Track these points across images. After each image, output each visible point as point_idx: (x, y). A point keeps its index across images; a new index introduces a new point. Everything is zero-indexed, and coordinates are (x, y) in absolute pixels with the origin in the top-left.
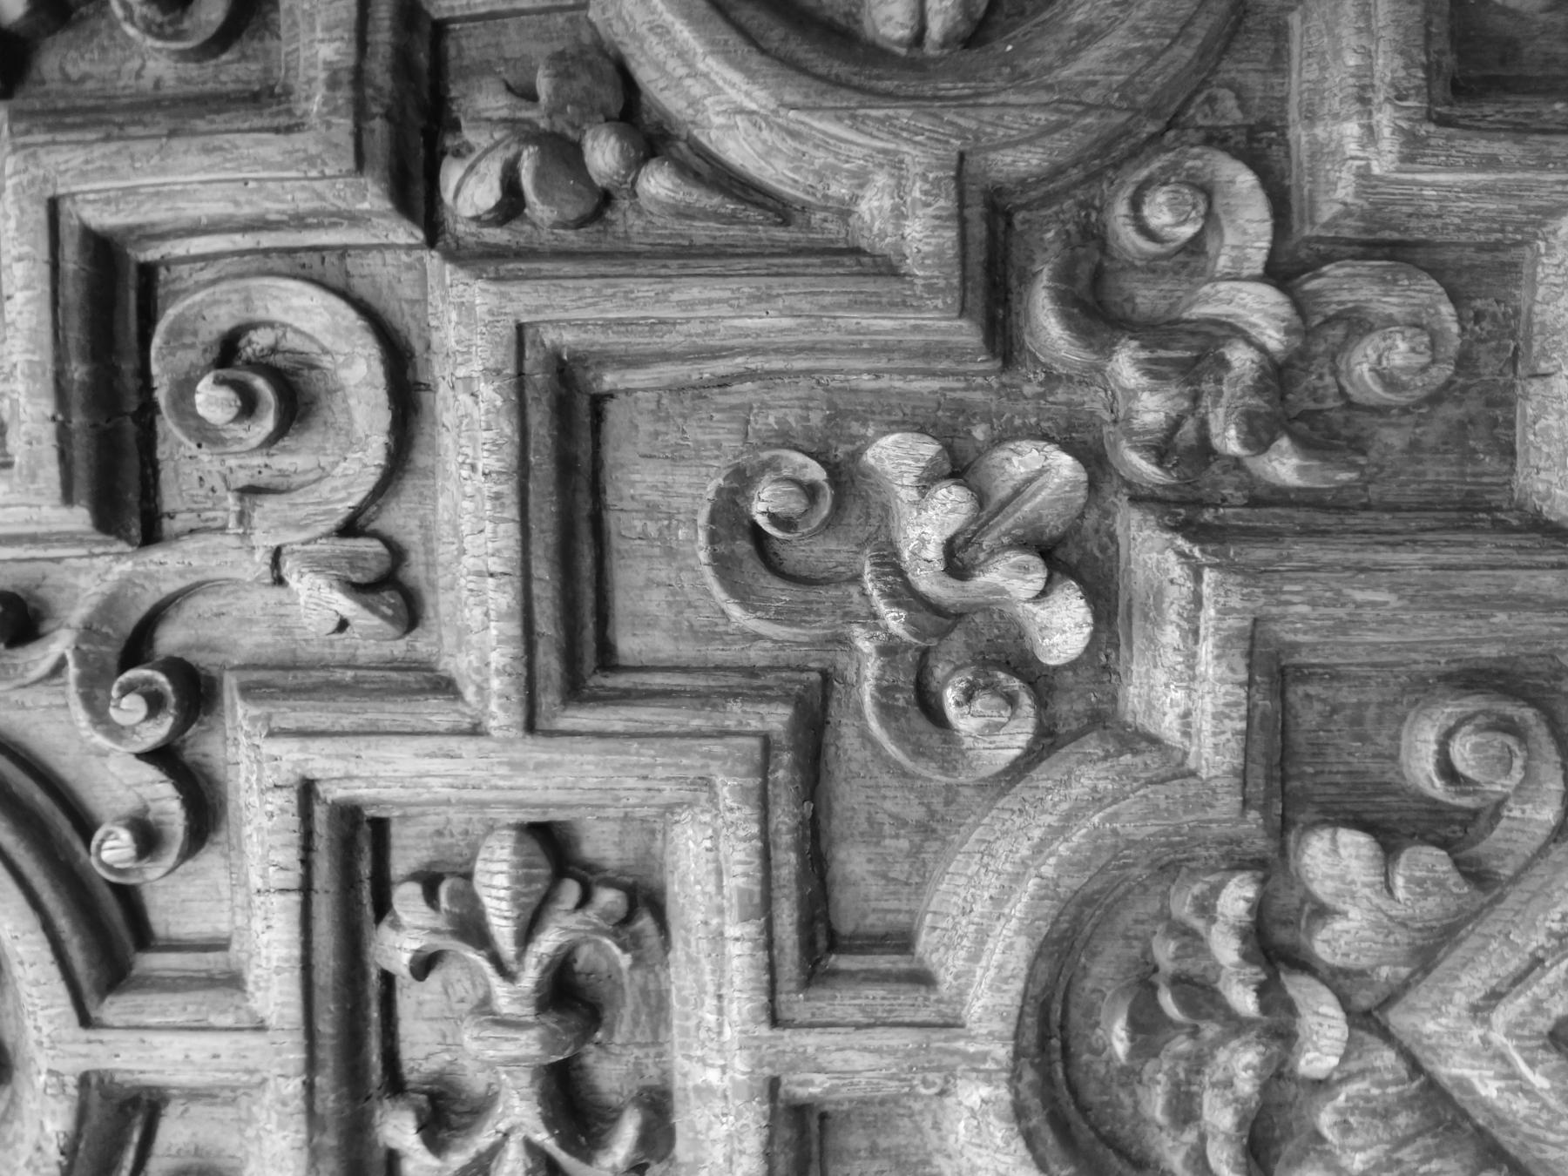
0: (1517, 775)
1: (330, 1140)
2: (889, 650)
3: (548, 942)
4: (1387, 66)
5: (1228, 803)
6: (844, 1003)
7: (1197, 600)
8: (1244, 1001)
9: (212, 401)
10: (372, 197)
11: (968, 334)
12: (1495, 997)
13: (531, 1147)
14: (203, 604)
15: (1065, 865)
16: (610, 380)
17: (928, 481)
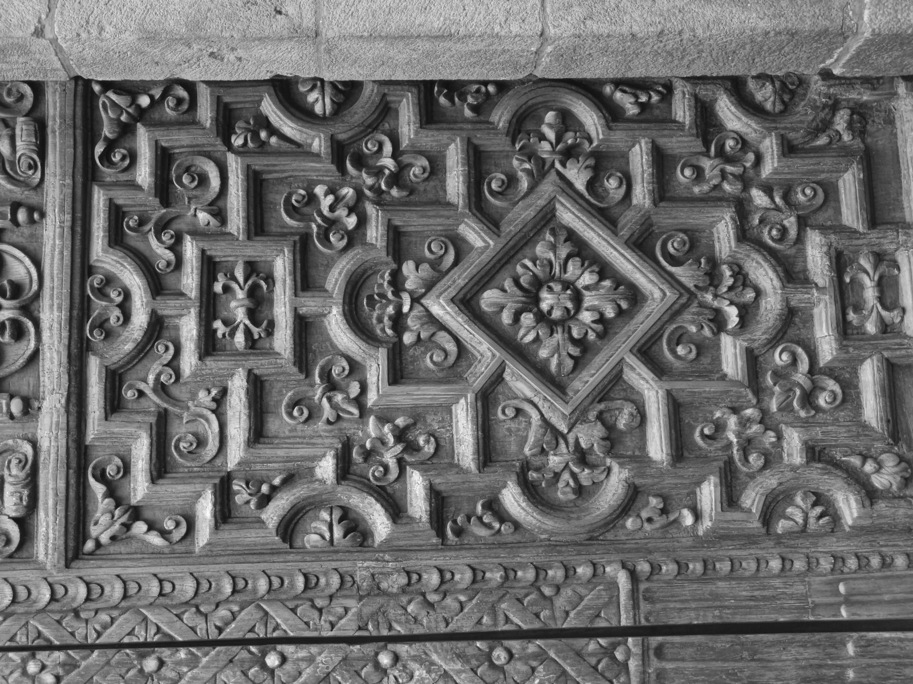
0: (443, 251)
1: (203, 323)
2: (319, 226)
3: (250, 282)
4: (412, 118)
5: (384, 254)
6: (309, 294)
7: (378, 216)
8: (390, 295)
9: (186, 179)
10: (219, 142)
11: (333, 167)
12: (441, 294)
13: (245, 324)
14: (178, 221)
15: (352, 265)
16: (265, 176)
17: (326, 195)
